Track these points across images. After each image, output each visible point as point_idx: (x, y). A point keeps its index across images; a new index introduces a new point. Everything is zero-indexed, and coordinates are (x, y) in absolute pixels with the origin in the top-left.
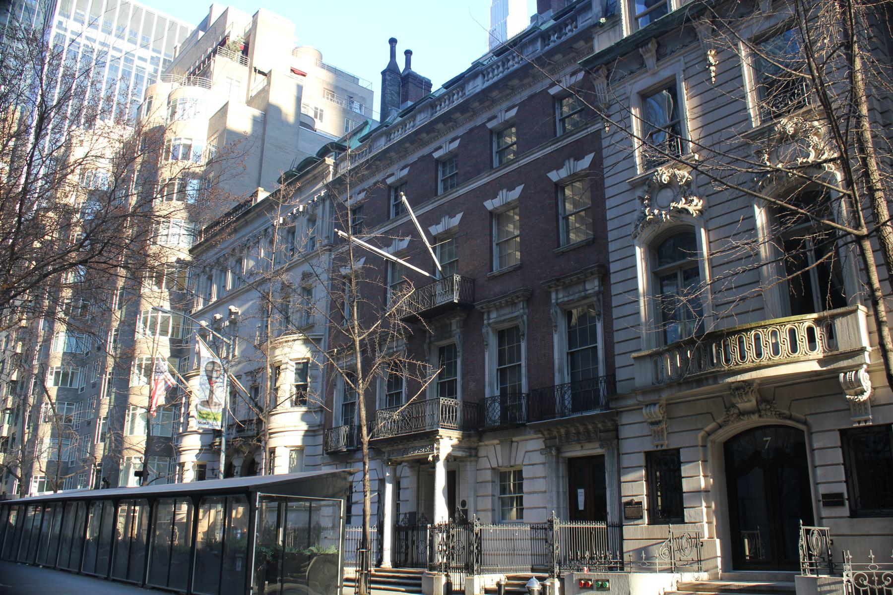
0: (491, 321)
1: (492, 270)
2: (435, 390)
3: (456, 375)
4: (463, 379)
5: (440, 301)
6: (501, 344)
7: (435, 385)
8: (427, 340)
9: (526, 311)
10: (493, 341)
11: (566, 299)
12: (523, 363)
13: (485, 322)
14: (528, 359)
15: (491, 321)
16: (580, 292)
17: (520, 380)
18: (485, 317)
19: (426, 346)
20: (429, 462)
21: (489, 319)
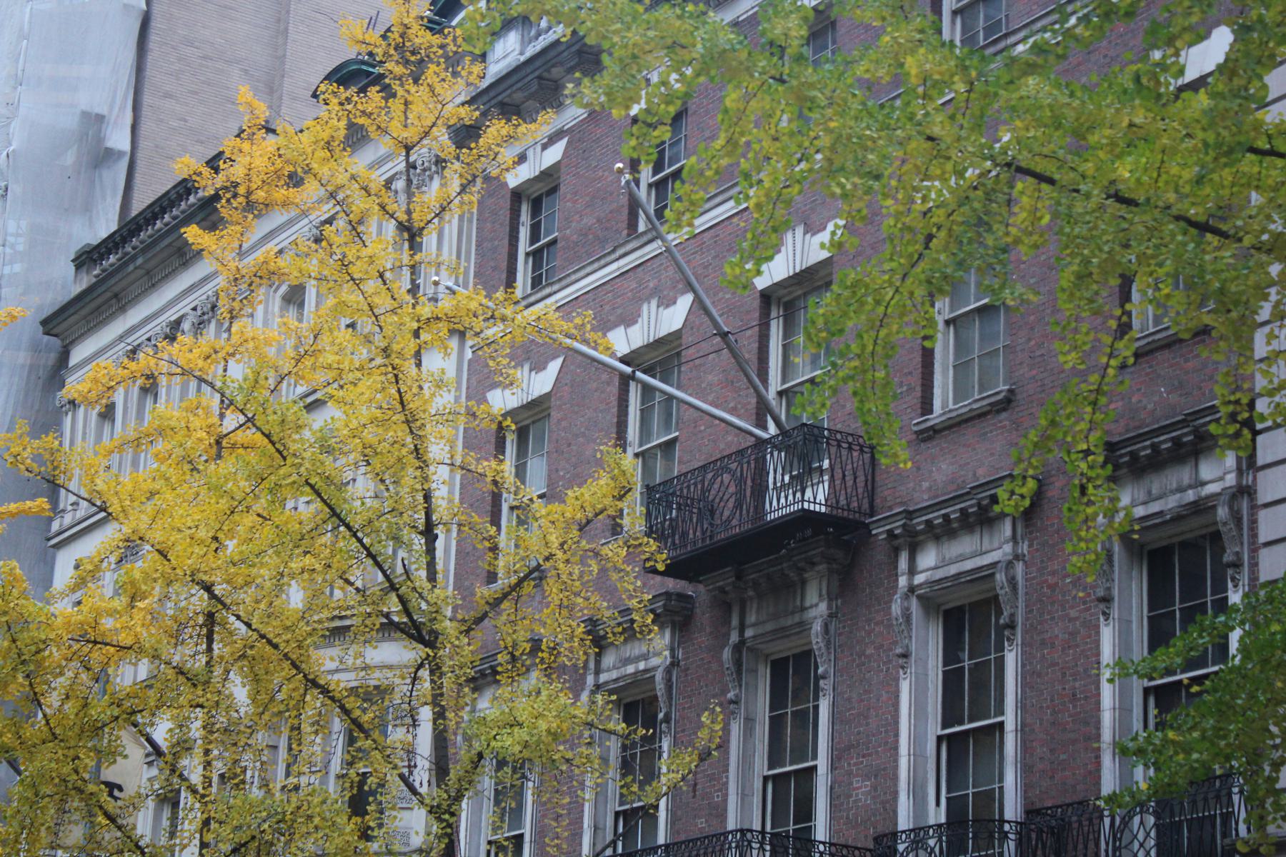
1: (927, 407)
2: (757, 800)
4: (833, 767)
5: (779, 506)
6: (951, 652)
7: (758, 784)
8: (734, 637)
9: (1024, 548)
10: (929, 644)
11: (1140, 511)
12: (1010, 719)
13: (903, 581)
14: (1022, 705)
15: (919, 579)
16: (1181, 490)
17: (1001, 779)
18: (903, 564)
19: (727, 654)
21: (912, 571)
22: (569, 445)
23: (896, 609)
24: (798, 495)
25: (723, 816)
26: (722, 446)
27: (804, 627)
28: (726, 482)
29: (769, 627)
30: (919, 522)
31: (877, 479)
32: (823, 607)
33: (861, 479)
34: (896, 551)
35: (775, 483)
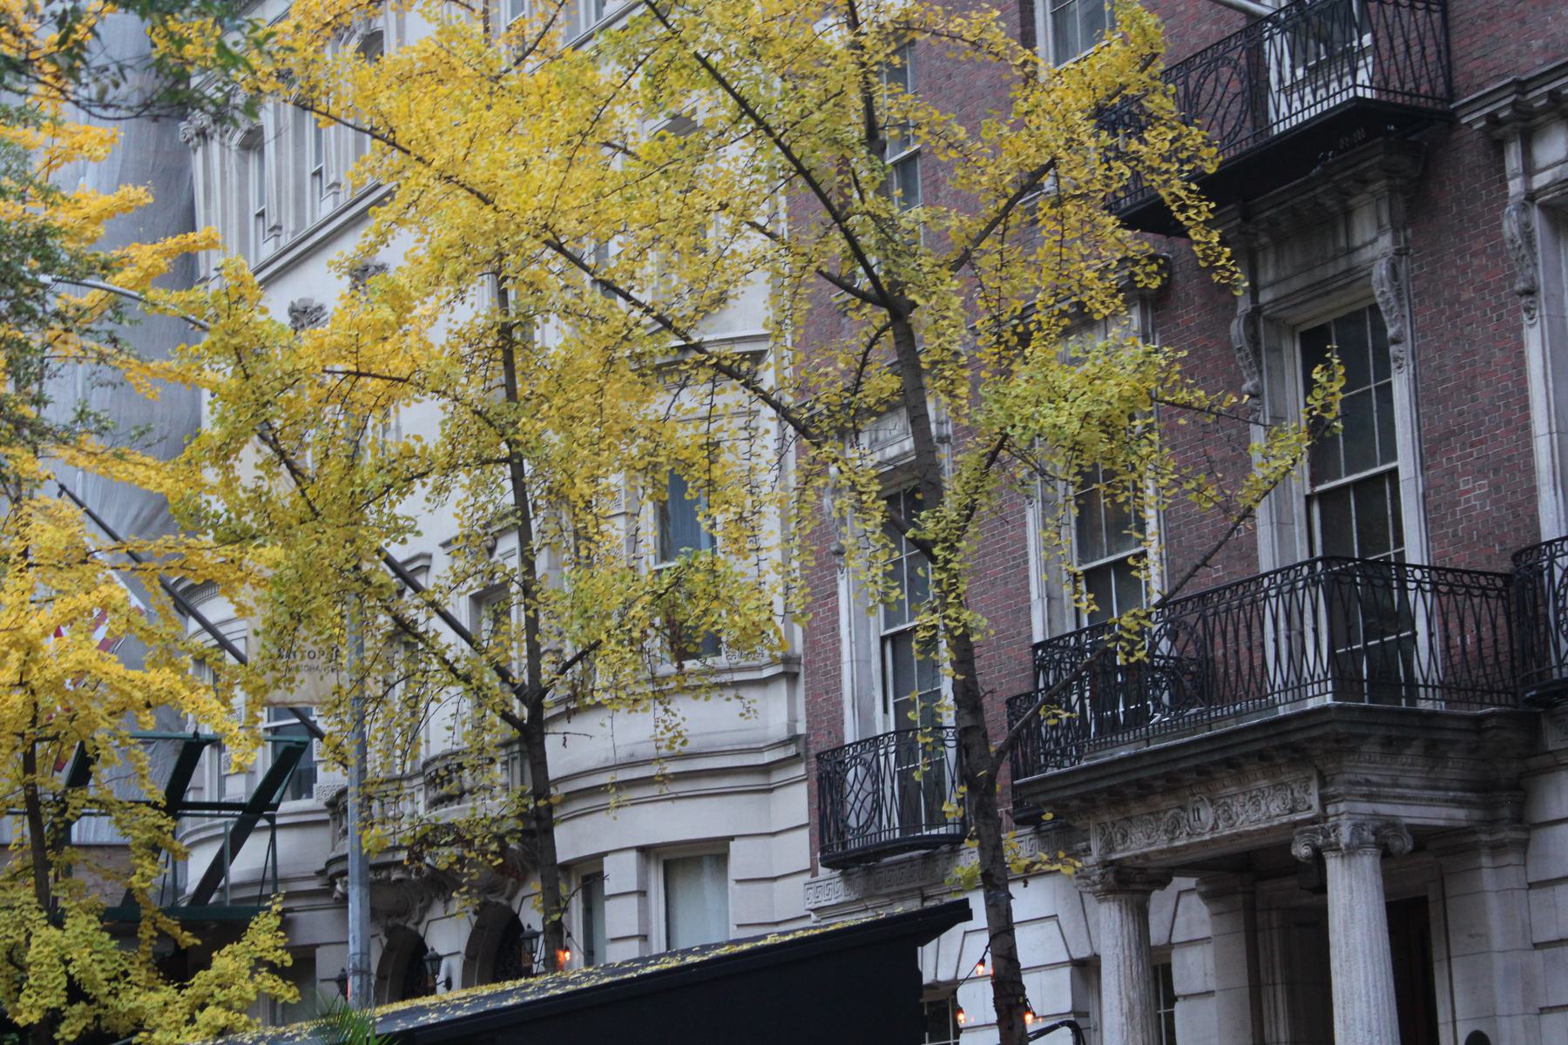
0: (1540, 181)
3: (1390, 453)
4: (1425, 464)
5: (1290, 110)
7: (1298, 507)
13: (1515, 187)
15: (1540, 181)
18: (1513, 161)
19: (1236, 328)
20: (1295, 866)
21: (1529, 170)
22: (949, 77)
23: (1510, 227)
24: (1348, 80)
25: (1251, 555)
26: (1193, 41)
27: (1356, 276)
28: (1224, 80)
29: (1297, 283)
30: (1538, 97)
31: (1454, 48)
32: (1386, 242)
33: (1431, 50)
34: (1499, 148)
35: (1281, 80)
